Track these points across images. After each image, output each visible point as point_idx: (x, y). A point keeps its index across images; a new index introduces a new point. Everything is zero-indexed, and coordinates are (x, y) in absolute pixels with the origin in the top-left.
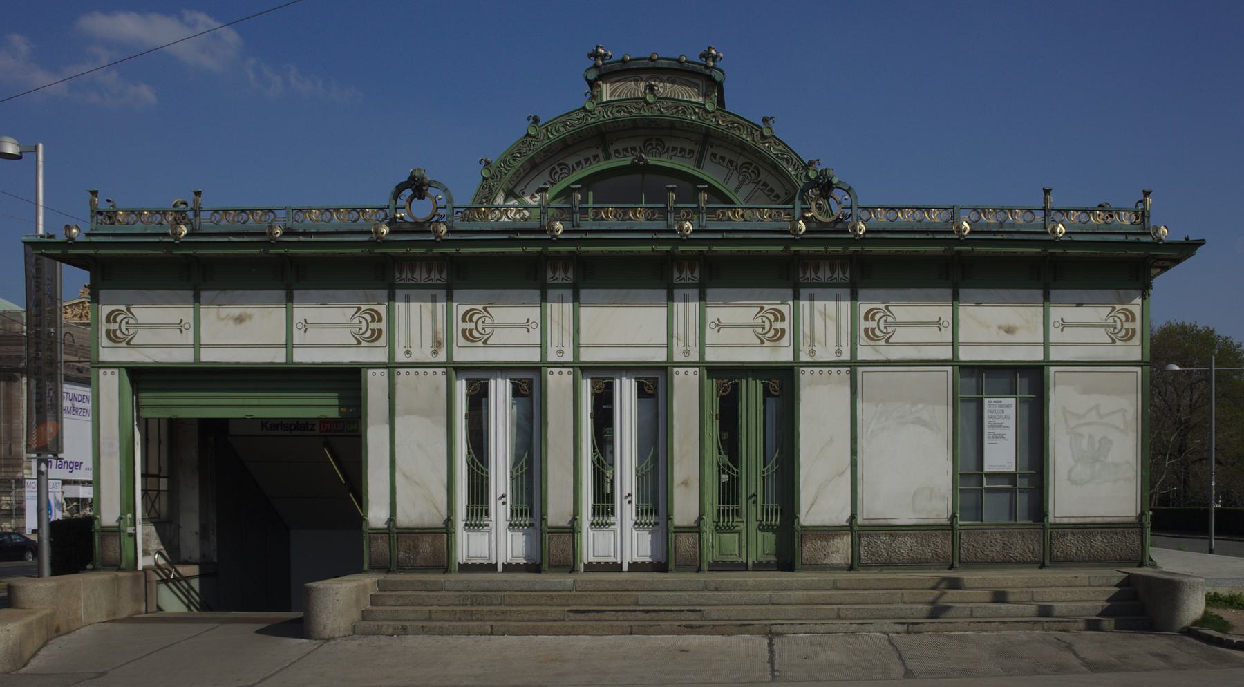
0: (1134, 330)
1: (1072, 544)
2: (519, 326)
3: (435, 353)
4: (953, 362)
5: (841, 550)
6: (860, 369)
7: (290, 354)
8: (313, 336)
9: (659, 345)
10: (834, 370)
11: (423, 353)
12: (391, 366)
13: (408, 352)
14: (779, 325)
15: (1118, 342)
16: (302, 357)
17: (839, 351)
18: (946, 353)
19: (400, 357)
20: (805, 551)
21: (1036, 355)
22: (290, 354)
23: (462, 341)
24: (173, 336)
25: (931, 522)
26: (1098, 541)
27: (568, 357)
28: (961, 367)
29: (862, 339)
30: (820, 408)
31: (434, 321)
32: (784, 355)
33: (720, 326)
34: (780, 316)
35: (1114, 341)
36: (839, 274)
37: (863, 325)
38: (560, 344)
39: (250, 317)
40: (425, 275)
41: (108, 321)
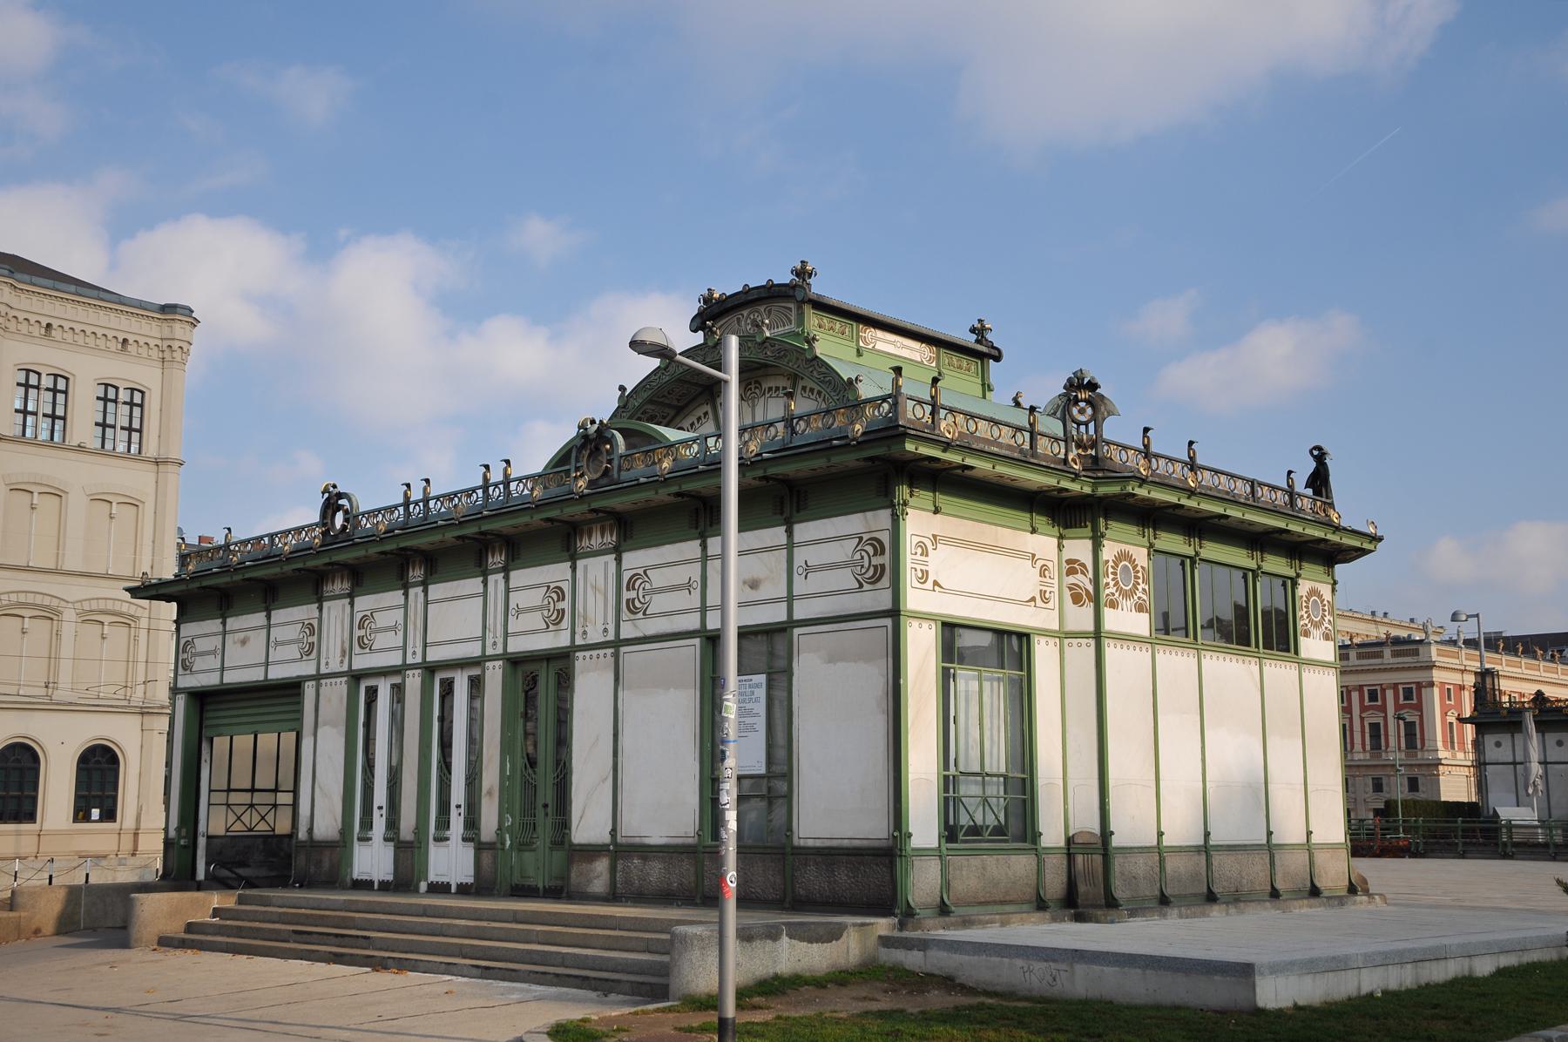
0: (883, 566)
1: (812, 880)
5: (599, 874)
6: (623, 649)
9: (475, 639)
10: (601, 652)
14: (560, 605)
15: (866, 587)
17: (605, 630)
19: (323, 670)
20: (573, 875)
25: (680, 841)
26: (843, 877)
27: (419, 659)
28: (708, 638)
34: (560, 593)
35: (861, 586)
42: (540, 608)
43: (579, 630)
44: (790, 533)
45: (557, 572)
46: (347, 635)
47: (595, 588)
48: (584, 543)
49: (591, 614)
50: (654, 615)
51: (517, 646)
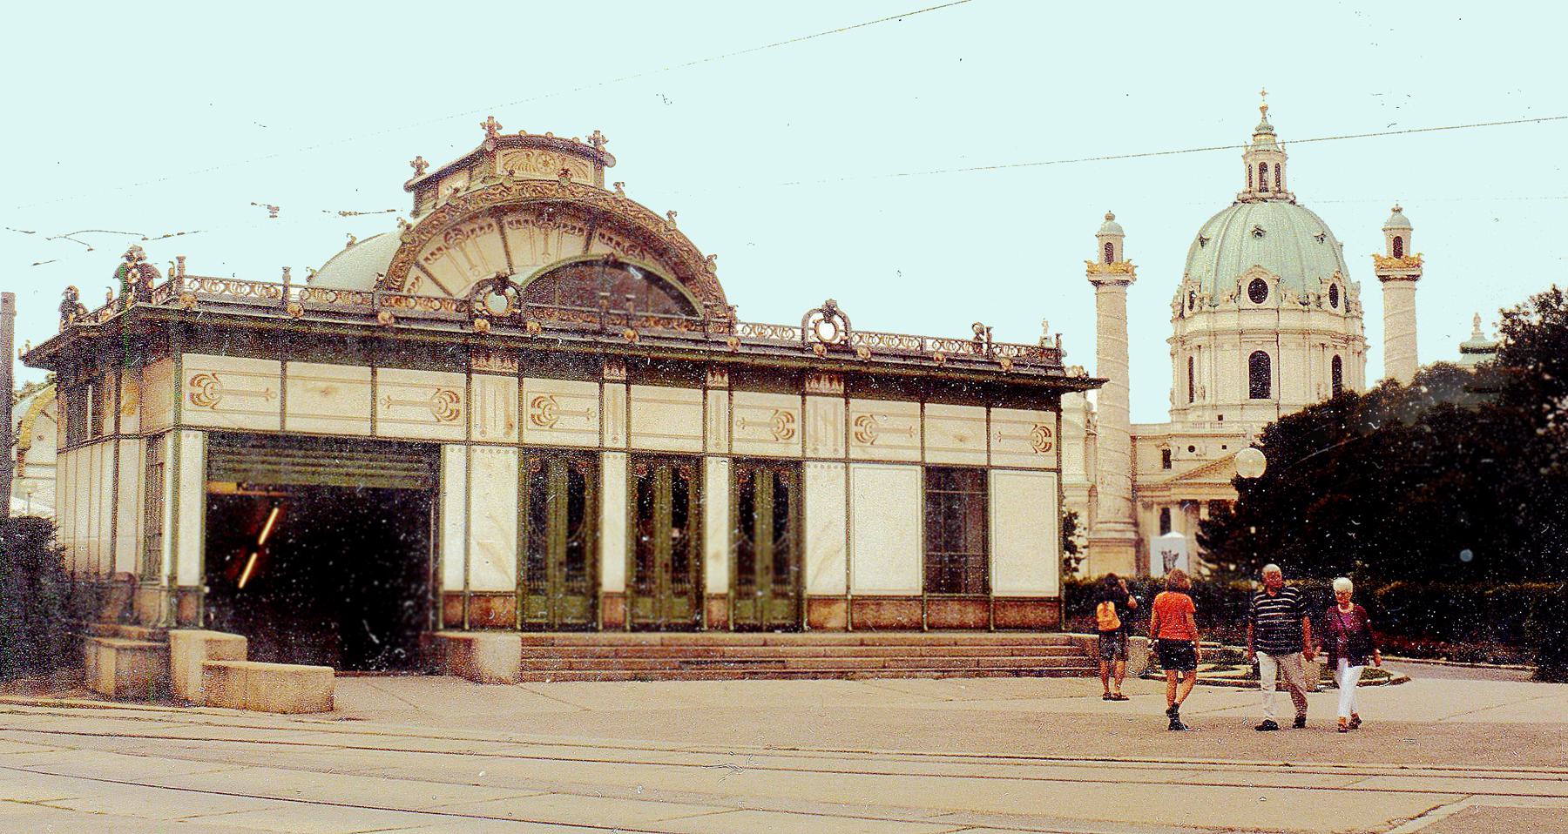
2: (578, 414)
3: (507, 434)
4: (922, 464)
5: (837, 616)
6: (852, 466)
7: (373, 428)
8: (397, 412)
9: (695, 438)
11: (496, 432)
12: (468, 443)
13: (483, 432)
14: (790, 426)
16: (386, 430)
18: (916, 456)
19: (476, 436)
21: (979, 460)
22: (373, 428)
23: (531, 425)
24: (259, 404)
29: (853, 440)
30: (821, 498)
31: (507, 403)
32: (794, 451)
33: (744, 424)
34: (790, 418)
36: (835, 385)
37: (853, 429)
38: (615, 432)
39: (336, 390)
40: (498, 362)
41: (192, 384)
42: (769, 425)
43: (809, 446)
44: (988, 412)
45: (790, 401)
46: (514, 409)
47: (825, 420)
48: (811, 385)
49: (821, 434)
50: (880, 446)
51: (741, 449)
